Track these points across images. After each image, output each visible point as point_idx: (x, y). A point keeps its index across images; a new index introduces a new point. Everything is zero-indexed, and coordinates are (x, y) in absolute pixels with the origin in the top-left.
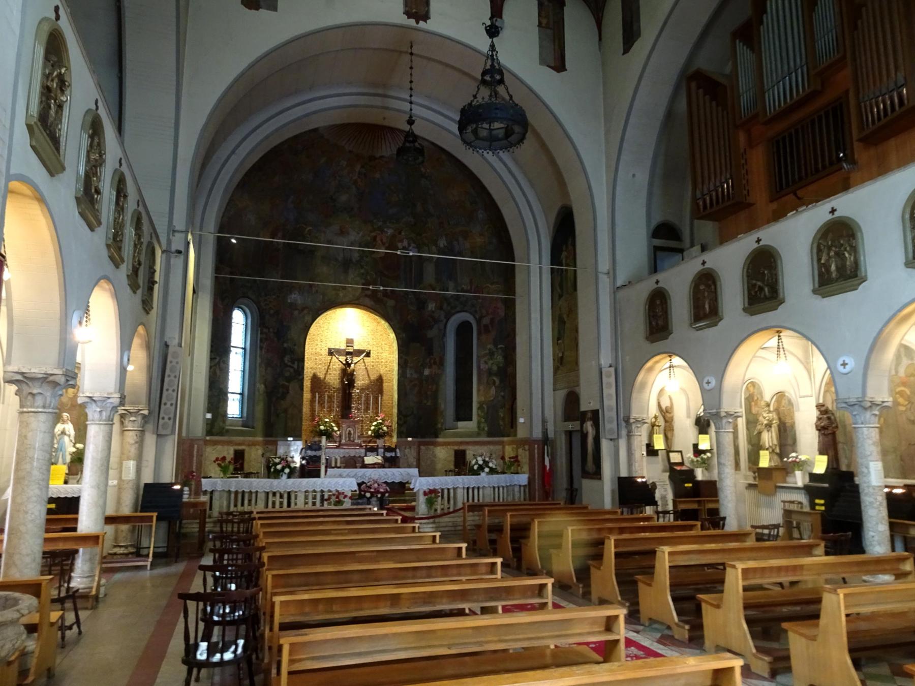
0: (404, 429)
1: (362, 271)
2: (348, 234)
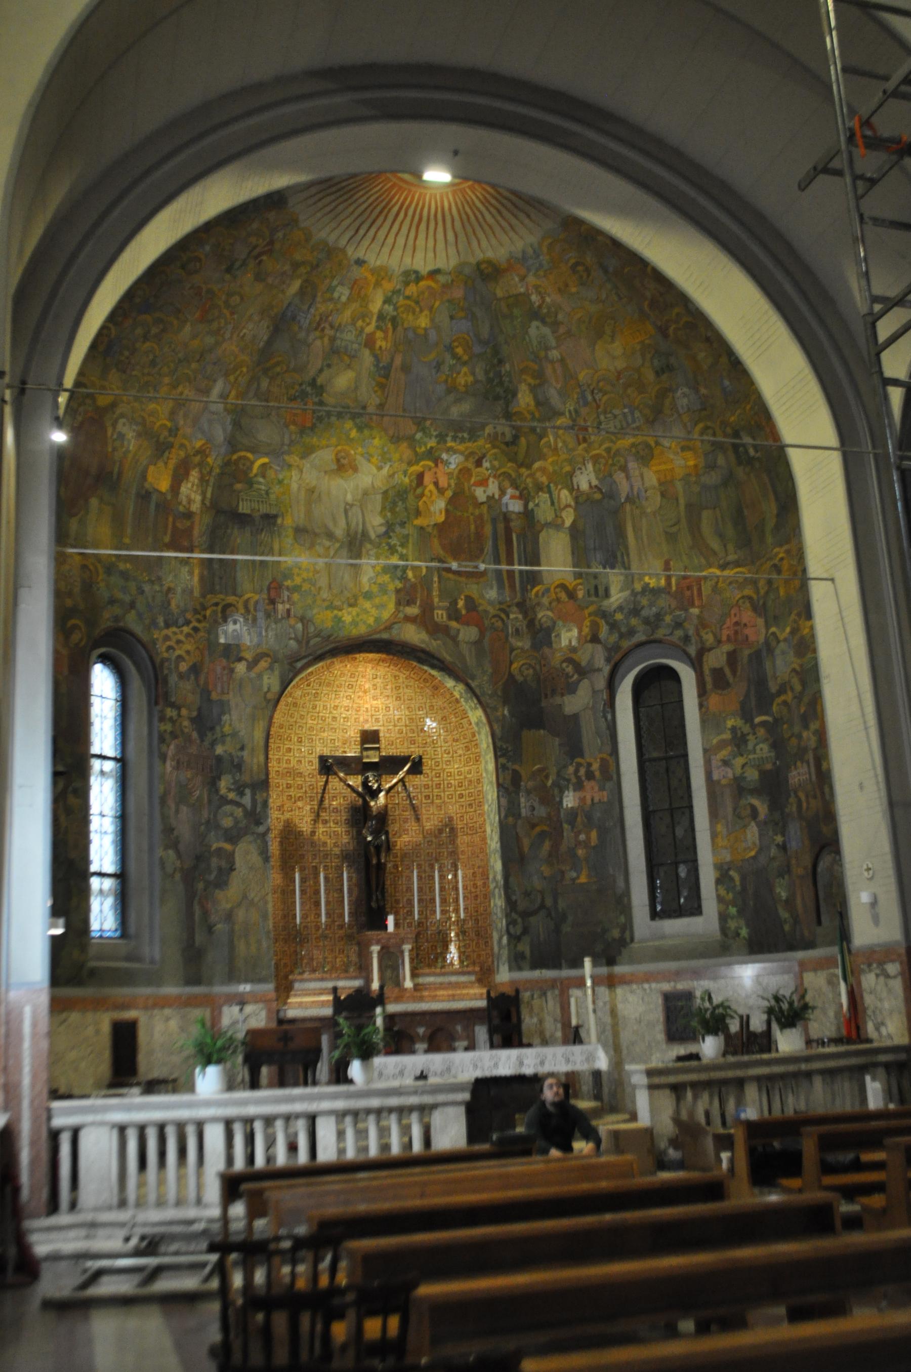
0: (524, 947)
2: (355, 469)
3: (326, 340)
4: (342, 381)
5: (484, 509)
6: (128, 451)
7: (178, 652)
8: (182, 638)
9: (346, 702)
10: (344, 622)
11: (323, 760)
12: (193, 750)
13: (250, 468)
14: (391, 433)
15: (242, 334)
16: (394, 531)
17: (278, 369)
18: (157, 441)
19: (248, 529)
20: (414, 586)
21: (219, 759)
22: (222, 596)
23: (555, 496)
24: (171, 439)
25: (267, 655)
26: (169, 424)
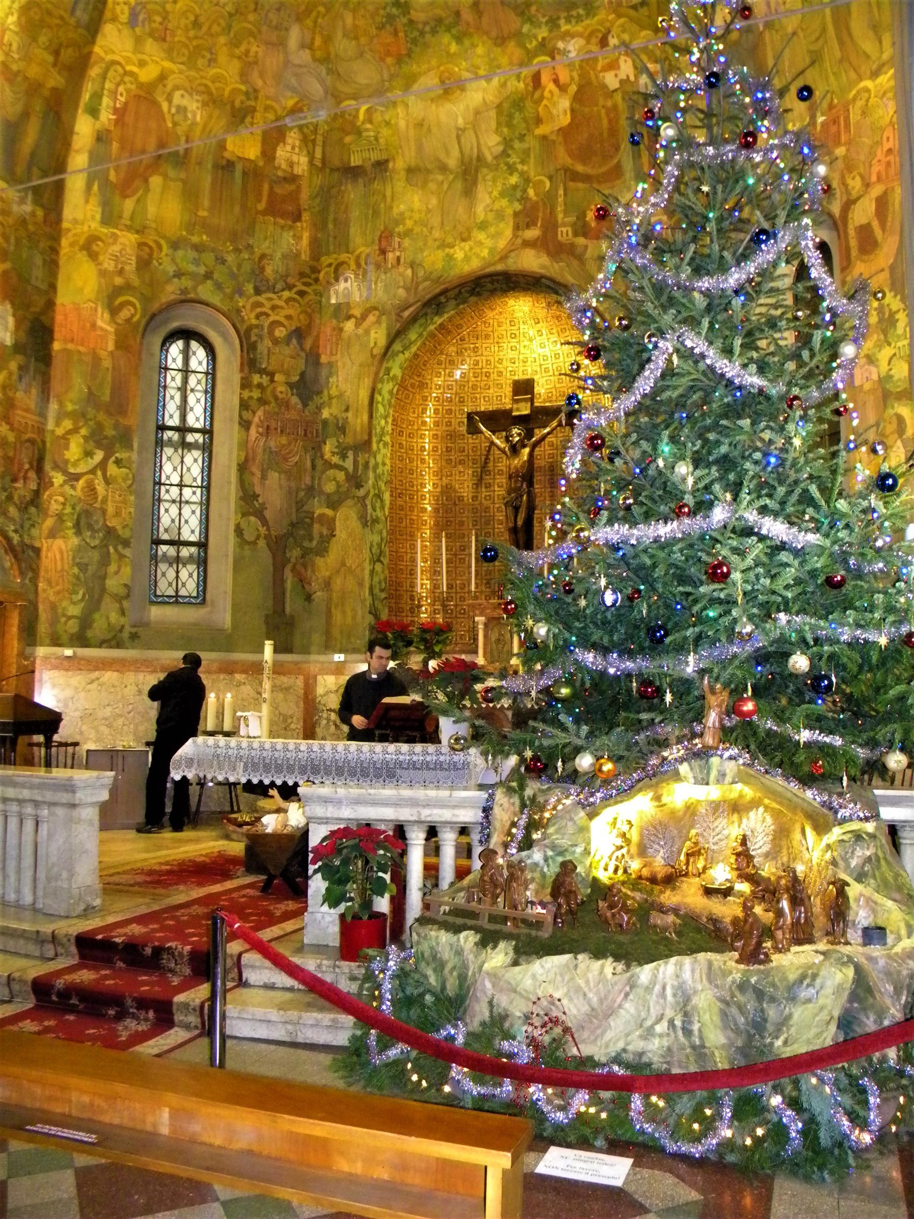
1: (514, 180)
5: (618, 97)
6: (194, 124)
7: (271, 319)
8: (281, 303)
9: (512, 354)
11: (470, 416)
12: (292, 415)
14: (494, 34)
16: (512, 148)
18: (233, 107)
19: (360, 181)
20: (535, 207)
21: (325, 422)
24: (252, 103)
25: (375, 309)
26: (243, 88)
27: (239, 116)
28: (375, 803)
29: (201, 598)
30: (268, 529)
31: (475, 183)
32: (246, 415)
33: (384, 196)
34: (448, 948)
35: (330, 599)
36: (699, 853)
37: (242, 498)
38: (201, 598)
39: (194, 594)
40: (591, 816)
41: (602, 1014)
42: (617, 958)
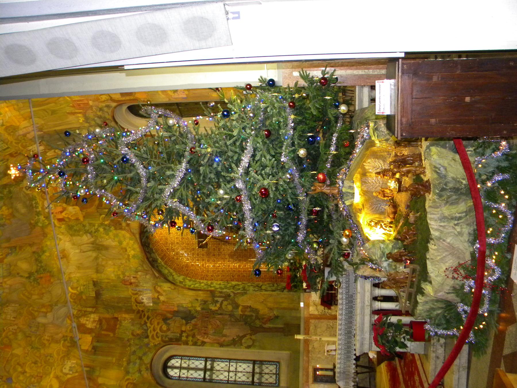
1: (101, 230)
2: (64, 250)
3: (5, 280)
4: (24, 266)
6: (77, 364)
7: (159, 331)
10: (134, 254)
12: (199, 323)
13: (75, 294)
14: (42, 238)
15: (14, 319)
16: (88, 230)
17: (27, 294)
18: (70, 346)
19: (101, 292)
21: (202, 309)
22: (133, 303)
23: (52, 157)
24: (68, 338)
25: (155, 288)
26: (62, 342)
27: (74, 344)
28: (363, 324)
29: (277, 363)
30: (248, 334)
31: (103, 245)
32: (199, 343)
33: (108, 282)
34: (425, 306)
35: (277, 308)
36: (383, 191)
37: (234, 346)
38: (277, 363)
39: (275, 366)
40: (368, 240)
41: (452, 250)
42: (428, 242)
